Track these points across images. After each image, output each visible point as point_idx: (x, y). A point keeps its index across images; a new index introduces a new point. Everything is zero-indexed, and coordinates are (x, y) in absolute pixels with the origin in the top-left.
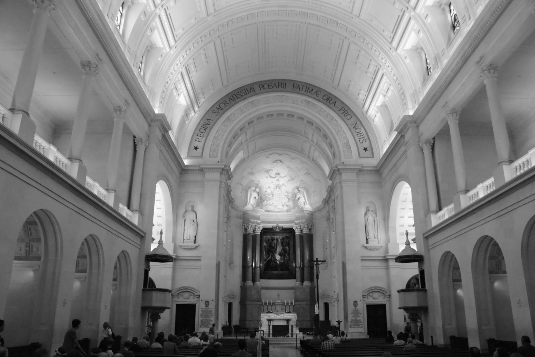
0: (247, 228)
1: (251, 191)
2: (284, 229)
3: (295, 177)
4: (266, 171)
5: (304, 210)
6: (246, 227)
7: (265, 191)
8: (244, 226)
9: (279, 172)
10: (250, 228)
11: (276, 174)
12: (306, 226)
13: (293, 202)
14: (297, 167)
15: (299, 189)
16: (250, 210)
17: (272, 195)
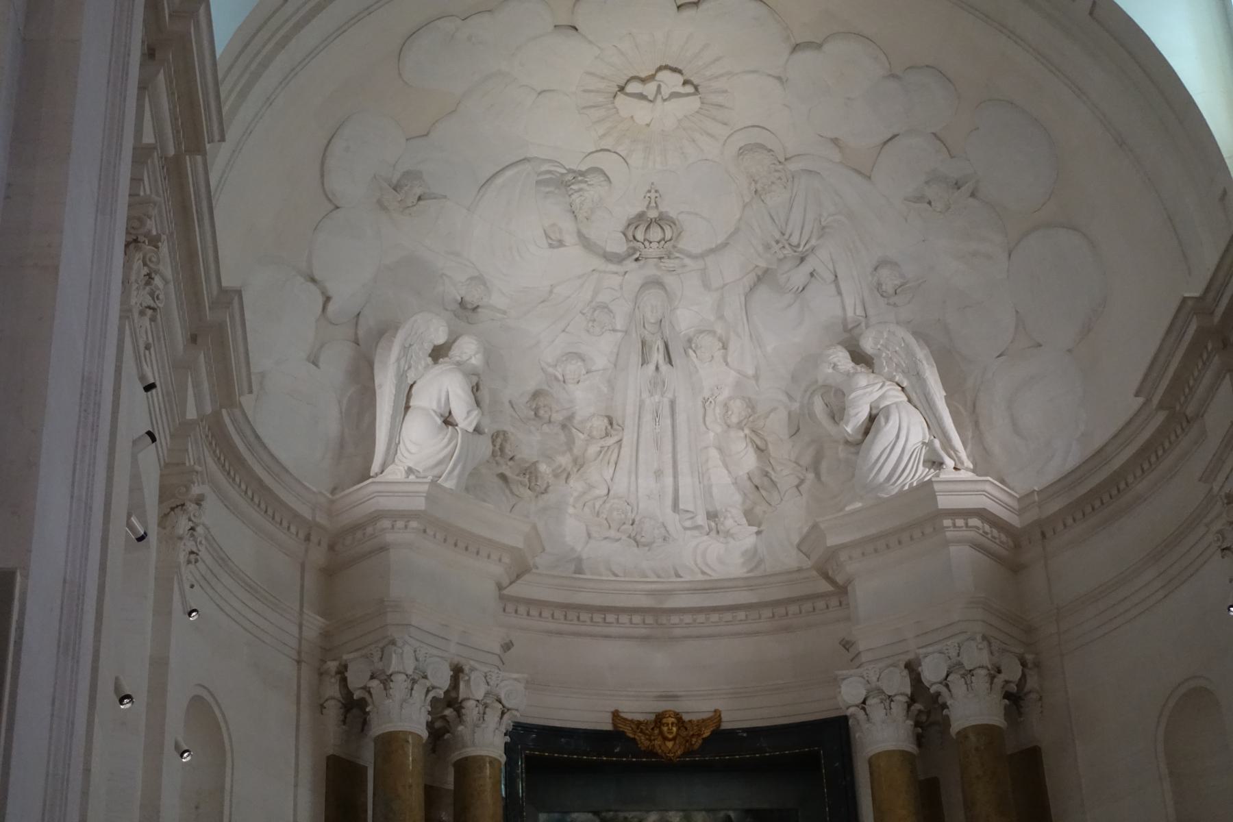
0: (375, 684)
1: (406, 349)
2: (732, 732)
3: (823, 231)
4: (538, 183)
5: (944, 502)
6: (356, 679)
7: (531, 386)
8: (342, 671)
9: (662, 208)
10: (400, 685)
11: (639, 219)
12: (977, 656)
13: (811, 476)
14: (835, 141)
15: (868, 345)
16: (407, 516)
17: (600, 423)
